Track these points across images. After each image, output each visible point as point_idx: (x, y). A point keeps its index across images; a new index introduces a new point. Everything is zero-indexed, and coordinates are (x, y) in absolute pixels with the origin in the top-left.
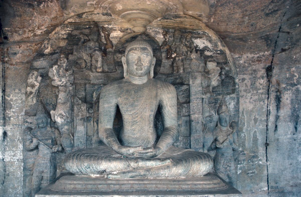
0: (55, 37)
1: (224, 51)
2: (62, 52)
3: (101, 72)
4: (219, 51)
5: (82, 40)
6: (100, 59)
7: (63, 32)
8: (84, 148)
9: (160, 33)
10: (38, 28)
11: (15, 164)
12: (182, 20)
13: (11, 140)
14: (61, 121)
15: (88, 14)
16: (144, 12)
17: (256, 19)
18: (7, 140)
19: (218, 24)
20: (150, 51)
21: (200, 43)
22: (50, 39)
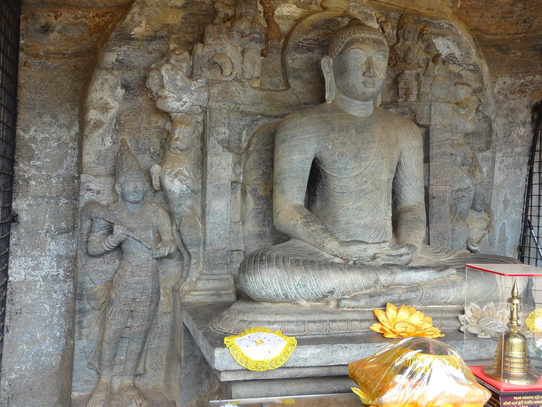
1: (480, 67)
2: (173, 36)
4: (472, 65)
5: (222, 15)
8: (226, 247)
9: (373, 17)
11: (38, 286)
13: (28, 232)
14: (180, 189)
17: (538, 8)
18: (18, 232)
19: (467, 12)
21: (443, 46)
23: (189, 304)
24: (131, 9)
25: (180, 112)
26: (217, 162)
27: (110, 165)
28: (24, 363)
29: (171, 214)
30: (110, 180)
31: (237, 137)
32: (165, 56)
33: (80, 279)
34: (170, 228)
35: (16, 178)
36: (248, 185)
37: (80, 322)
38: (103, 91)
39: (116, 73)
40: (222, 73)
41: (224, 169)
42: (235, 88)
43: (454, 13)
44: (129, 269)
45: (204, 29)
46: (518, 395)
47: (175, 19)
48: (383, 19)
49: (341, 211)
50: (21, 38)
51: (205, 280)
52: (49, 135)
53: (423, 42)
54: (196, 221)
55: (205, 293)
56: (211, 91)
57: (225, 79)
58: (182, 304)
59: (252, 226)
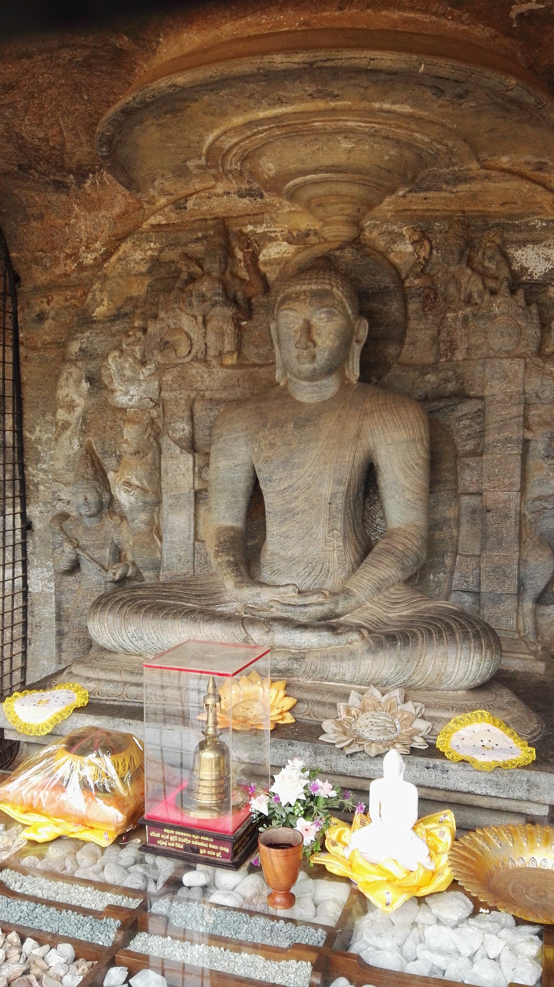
0: (119, 270)
2: (138, 311)
3: (232, 366)
5: (184, 276)
6: (229, 328)
7: (138, 255)
9: (404, 236)
10: (87, 247)
12: (475, 187)
15: (201, 198)
16: (342, 175)
20: (342, 302)
22: (105, 276)
25: (131, 408)
35: (27, 483)
38: (68, 386)
39: (80, 364)
46: (171, 827)
50: (20, 331)
56: (164, 379)
57: (180, 361)
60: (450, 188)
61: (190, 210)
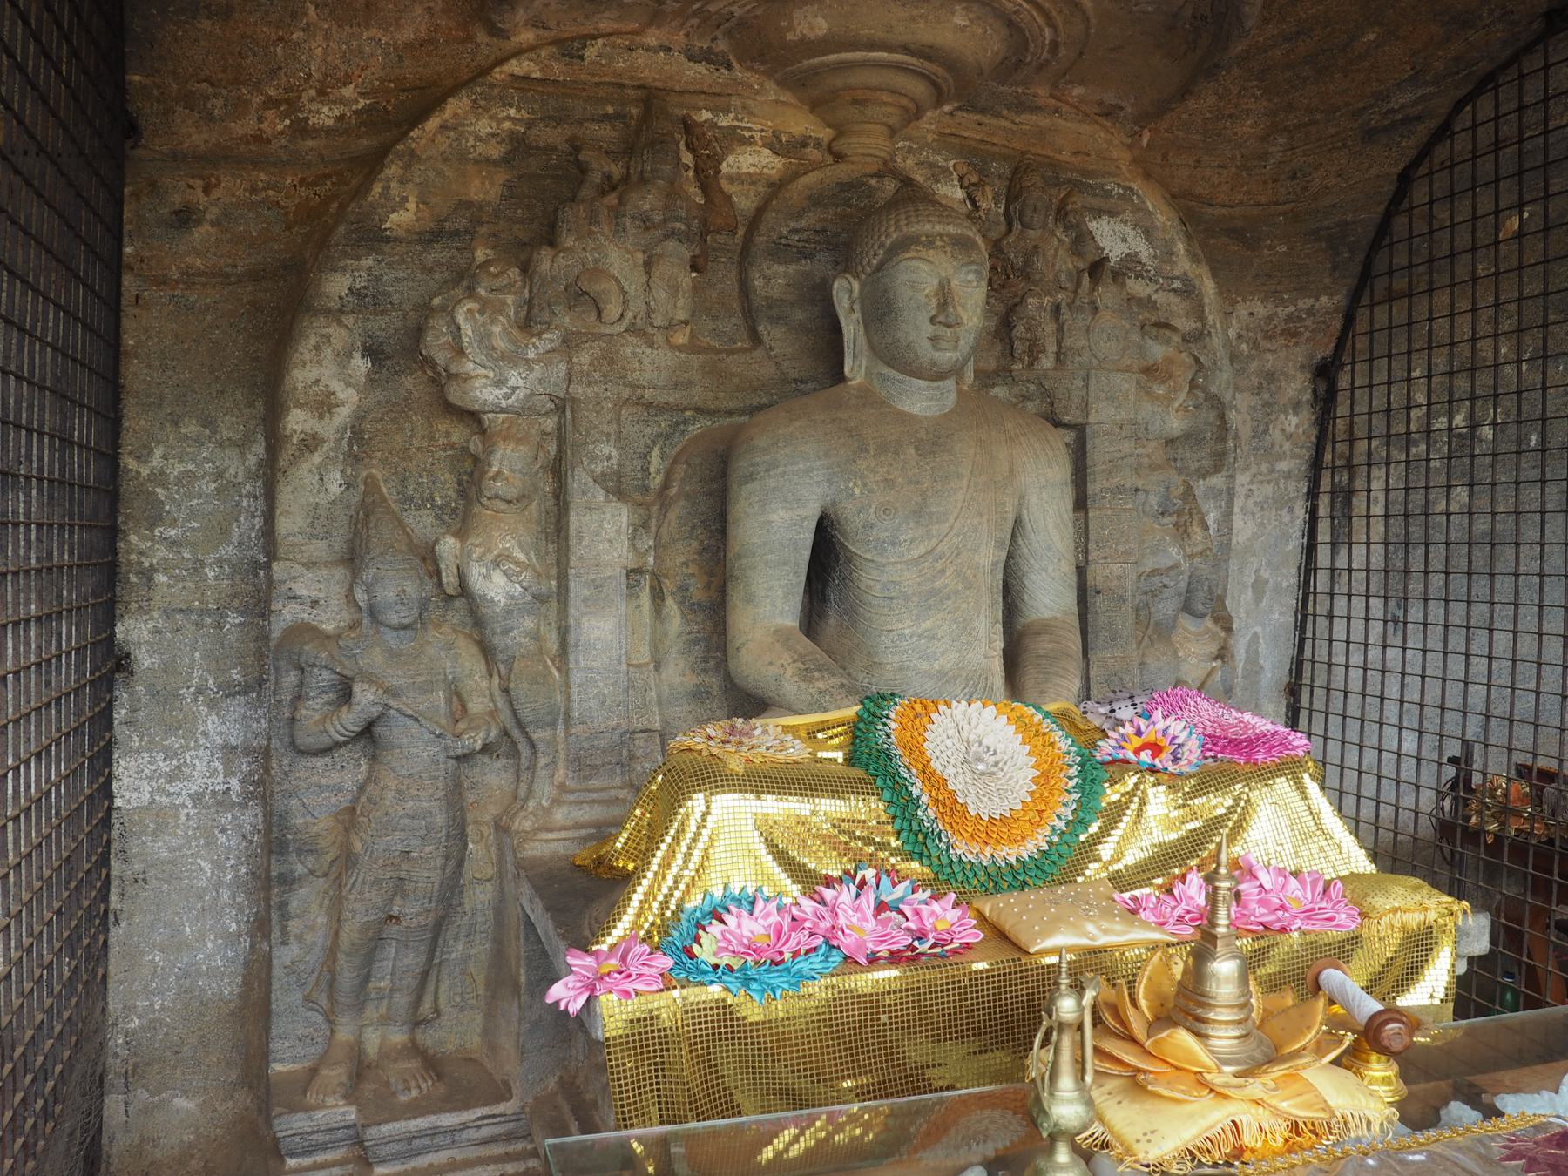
2: (483, 230)
4: (1178, 278)
5: (596, 177)
7: (484, 126)
10: (322, 92)
11: (183, 818)
12: (1044, 121)
13: (154, 694)
18: (131, 695)
19: (1165, 157)
21: (1112, 238)
22: (412, 153)
23: (534, 863)
24: (381, 170)
25: (503, 411)
26: (594, 526)
27: (339, 542)
28: (159, 992)
29: (487, 651)
30: (340, 573)
31: (638, 464)
32: (464, 278)
33: (279, 805)
34: (485, 684)
35: (123, 569)
36: (666, 576)
37: (283, 905)
38: (319, 363)
39: (349, 320)
40: (599, 316)
41: (610, 541)
42: (631, 348)
43: (1134, 161)
44: (393, 785)
45: (556, 210)
47: (484, 189)
48: (974, 179)
49: (885, 640)
50: (126, 240)
51: (571, 803)
52: (197, 465)
53: (1066, 229)
54: (546, 666)
55: (570, 834)
56: (575, 360)
58: (520, 865)
59: (678, 673)
60: (1012, 115)
61: (592, 63)
